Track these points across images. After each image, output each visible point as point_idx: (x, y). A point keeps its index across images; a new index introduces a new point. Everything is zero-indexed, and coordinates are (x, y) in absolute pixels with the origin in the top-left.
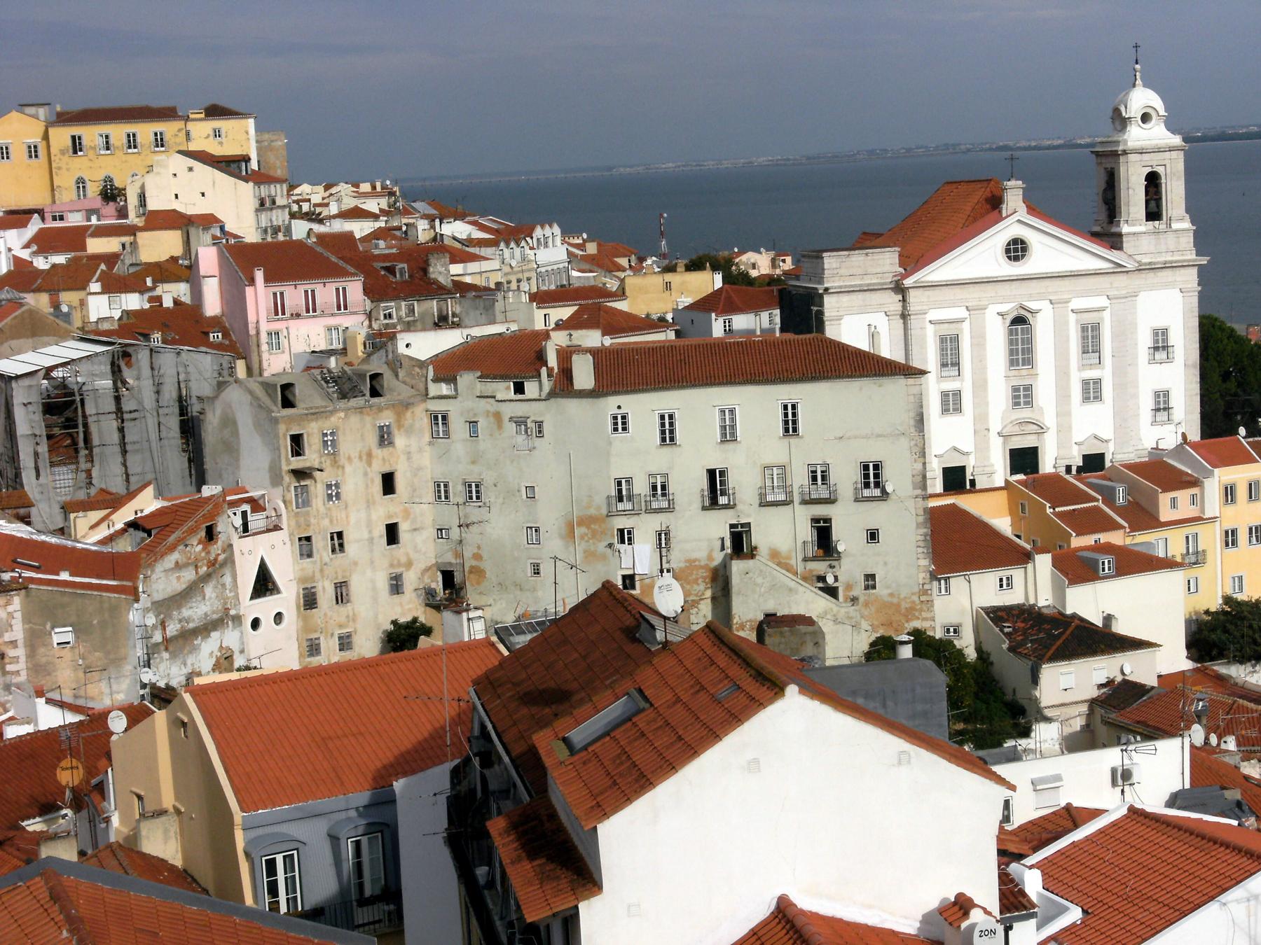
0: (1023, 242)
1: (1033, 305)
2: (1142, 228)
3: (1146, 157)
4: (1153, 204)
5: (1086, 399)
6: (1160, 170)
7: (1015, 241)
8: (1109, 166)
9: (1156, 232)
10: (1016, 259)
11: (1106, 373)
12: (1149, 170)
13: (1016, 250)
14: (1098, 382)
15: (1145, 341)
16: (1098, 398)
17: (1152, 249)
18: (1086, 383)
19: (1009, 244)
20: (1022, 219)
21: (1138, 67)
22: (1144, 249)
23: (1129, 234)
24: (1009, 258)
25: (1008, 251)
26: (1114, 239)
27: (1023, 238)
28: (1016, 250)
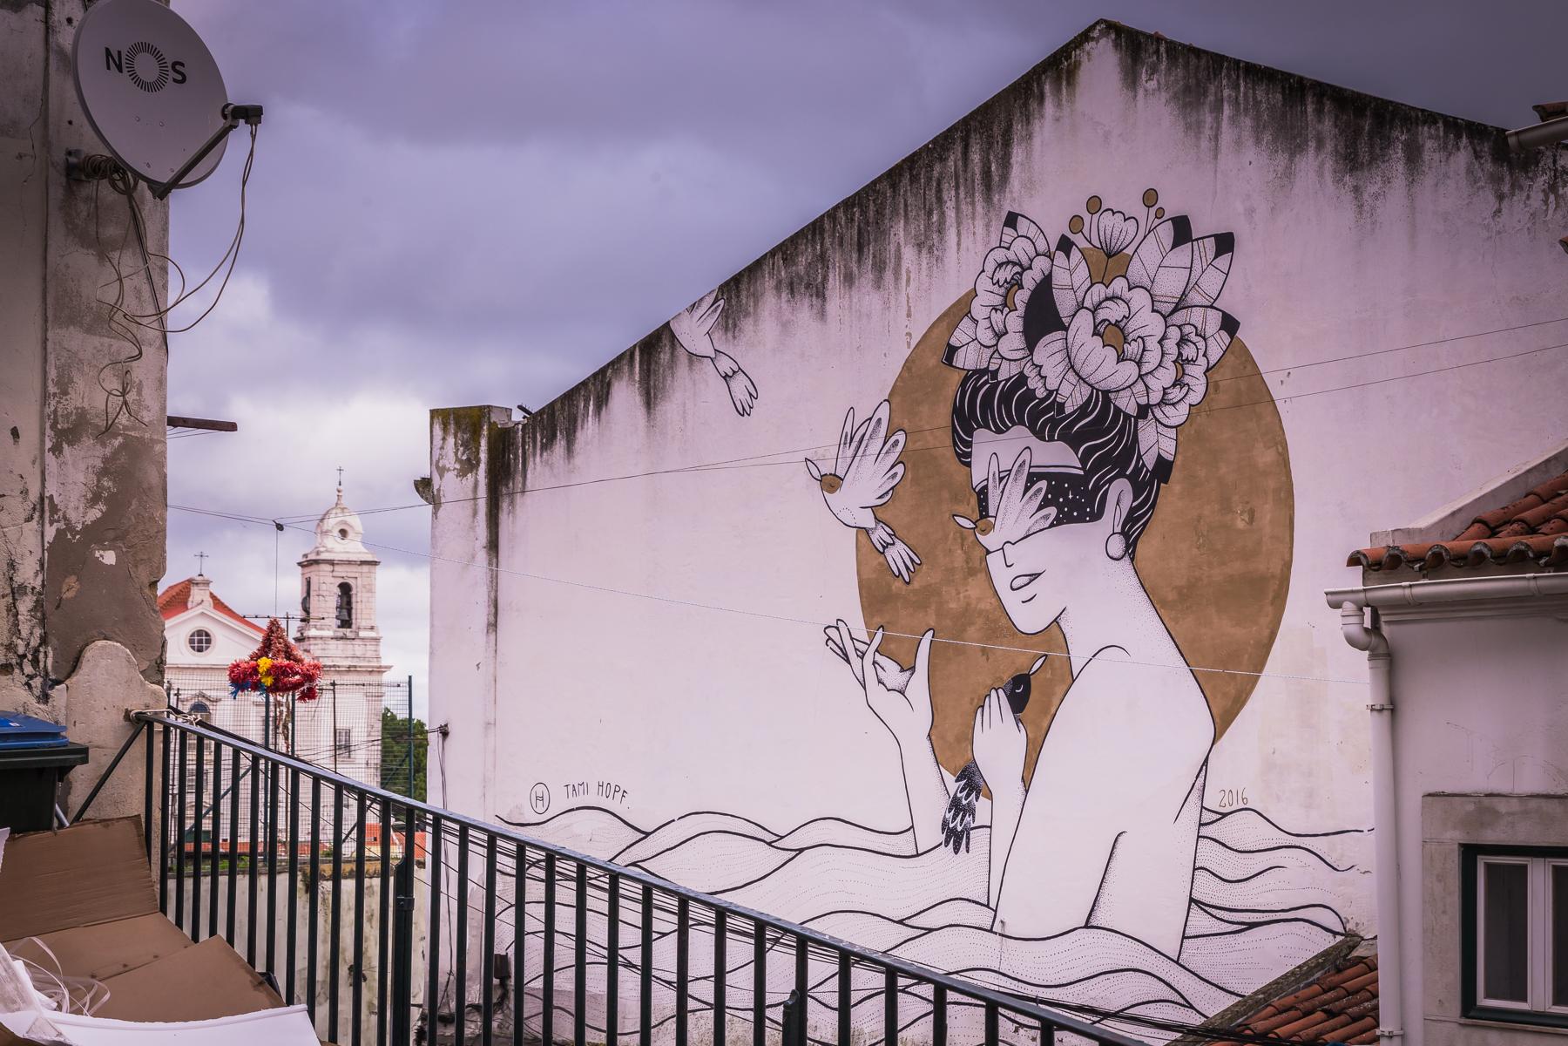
0: (207, 635)
1: (213, 694)
2: (330, 633)
3: (337, 568)
4: (345, 612)
6: (352, 582)
7: (200, 633)
8: (307, 576)
9: (344, 638)
10: (200, 650)
12: (341, 581)
13: (200, 641)
17: (339, 653)
19: (193, 635)
20: (206, 612)
22: (329, 653)
23: (315, 638)
25: (191, 642)
27: (207, 630)
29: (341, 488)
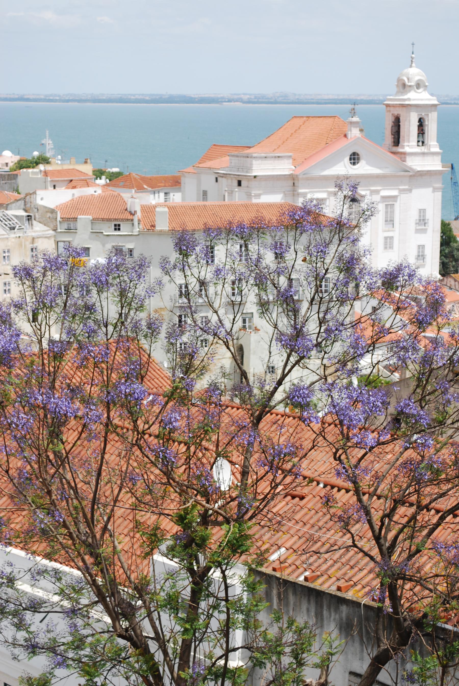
0: (358, 155)
5: (386, 248)
8: (396, 113)
10: (354, 164)
11: (395, 234)
13: (354, 159)
14: (392, 238)
15: (414, 216)
16: (391, 247)
18: (386, 238)
19: (351, 156)
21: (413, 56)
24: (351, 163)
26: (403, 156)
28: (354, 159)
29: (413, 56)
